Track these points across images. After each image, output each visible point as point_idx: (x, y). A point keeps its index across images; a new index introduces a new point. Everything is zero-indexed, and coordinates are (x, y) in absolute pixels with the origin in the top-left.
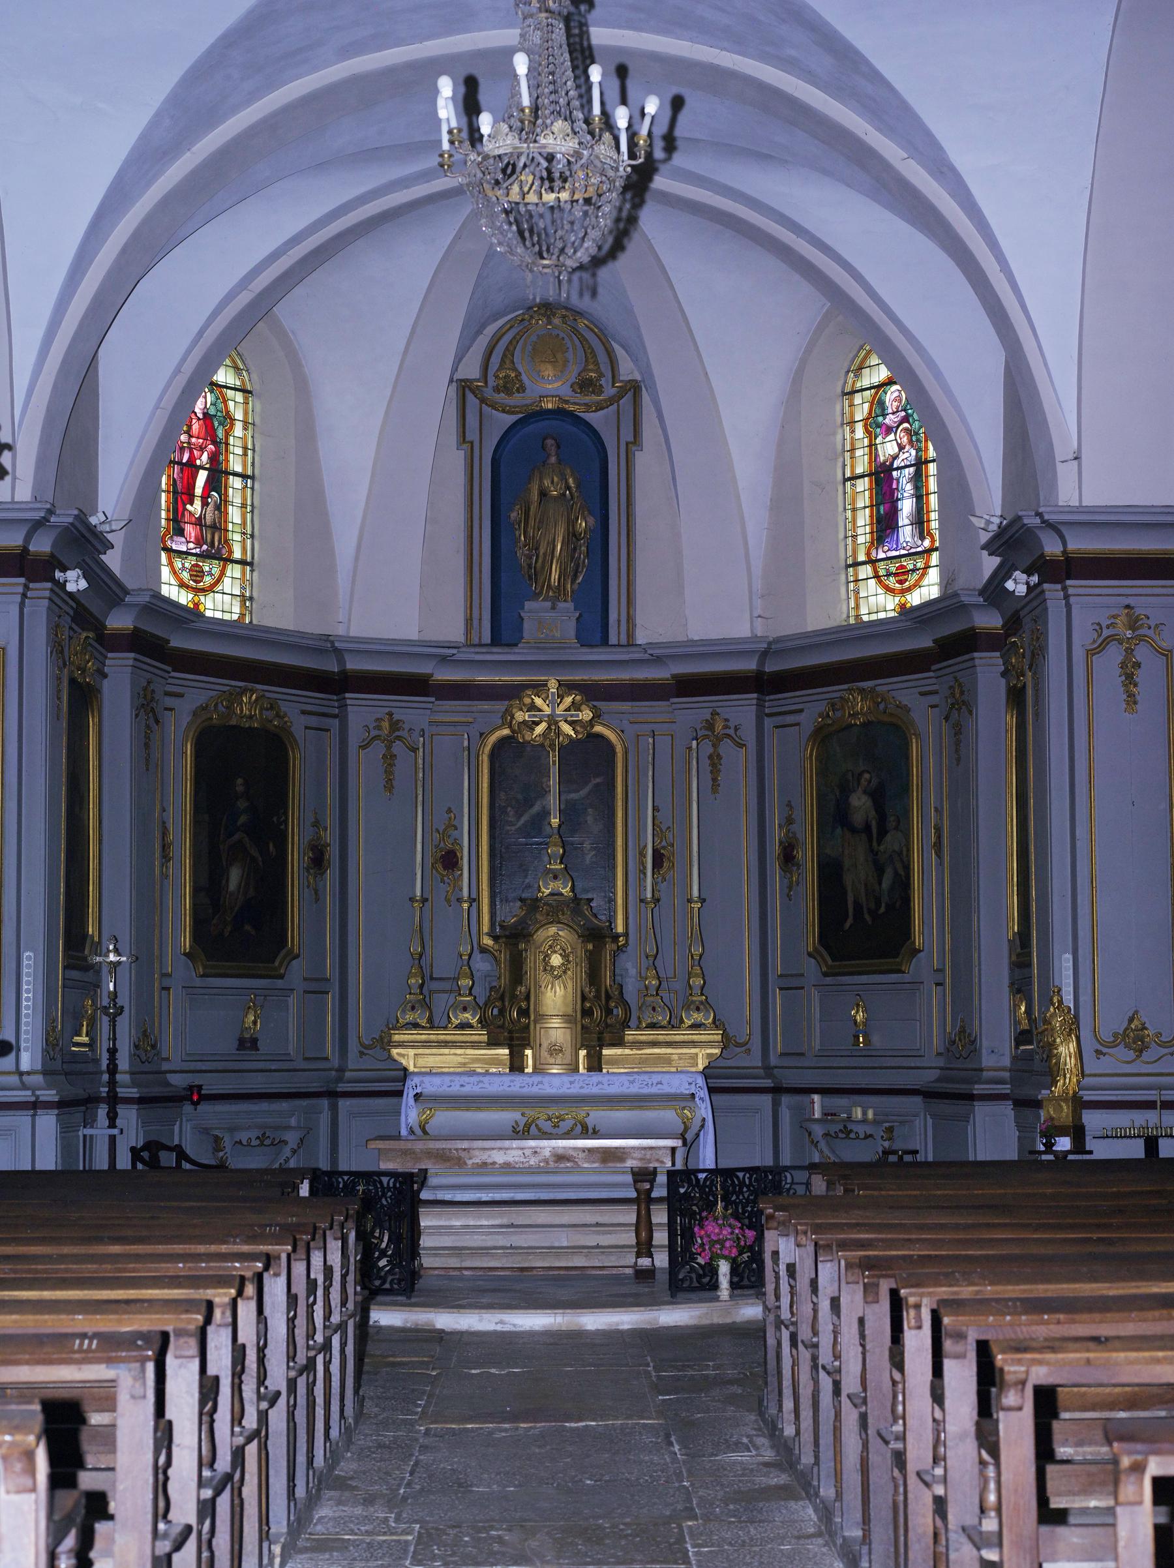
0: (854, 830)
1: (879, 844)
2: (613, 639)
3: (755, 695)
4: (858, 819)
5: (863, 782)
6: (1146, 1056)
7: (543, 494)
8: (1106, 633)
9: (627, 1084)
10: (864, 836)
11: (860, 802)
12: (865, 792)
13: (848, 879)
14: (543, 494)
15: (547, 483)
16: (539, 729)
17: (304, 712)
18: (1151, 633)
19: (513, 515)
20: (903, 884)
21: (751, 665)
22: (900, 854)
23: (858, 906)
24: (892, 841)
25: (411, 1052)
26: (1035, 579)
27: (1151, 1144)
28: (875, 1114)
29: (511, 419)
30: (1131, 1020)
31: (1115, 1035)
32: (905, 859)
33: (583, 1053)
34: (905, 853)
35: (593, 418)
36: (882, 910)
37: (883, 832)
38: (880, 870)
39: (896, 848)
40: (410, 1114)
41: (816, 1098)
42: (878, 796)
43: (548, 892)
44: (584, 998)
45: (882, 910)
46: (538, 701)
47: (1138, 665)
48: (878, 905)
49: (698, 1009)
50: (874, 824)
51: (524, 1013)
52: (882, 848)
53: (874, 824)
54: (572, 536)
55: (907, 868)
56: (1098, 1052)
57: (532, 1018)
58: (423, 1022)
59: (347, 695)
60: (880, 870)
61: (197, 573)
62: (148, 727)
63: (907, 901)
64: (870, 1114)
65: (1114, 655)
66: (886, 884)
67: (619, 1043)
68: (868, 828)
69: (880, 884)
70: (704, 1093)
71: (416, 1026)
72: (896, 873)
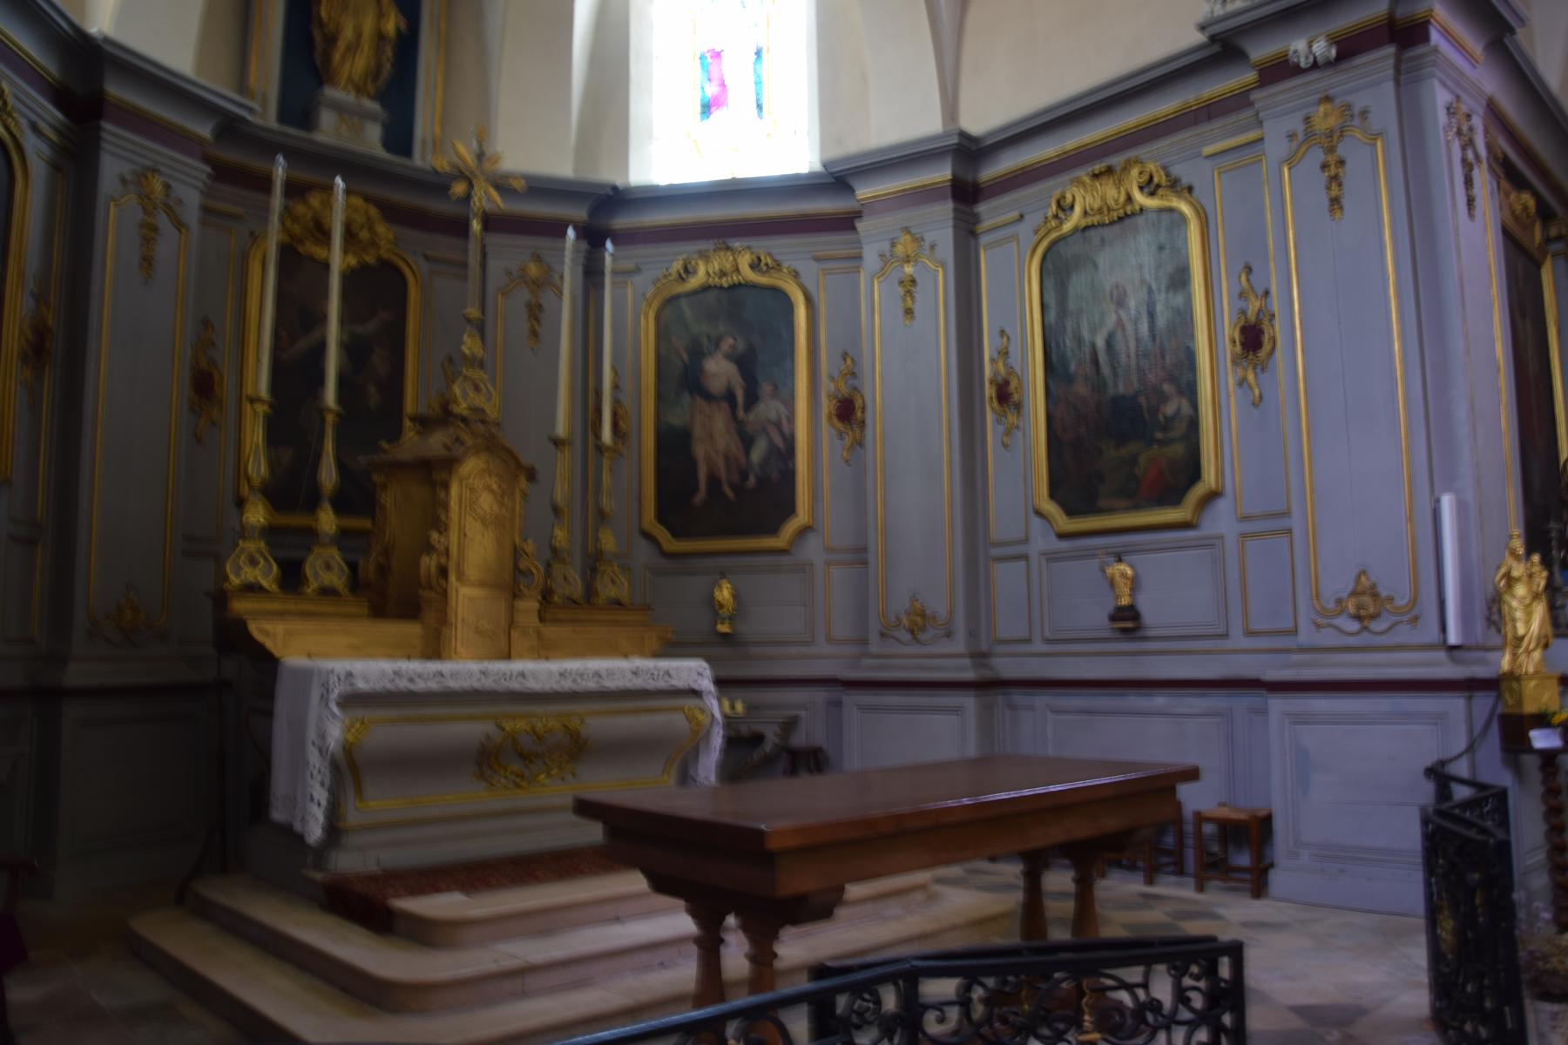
0: (708, 397)
4: (716, 385)
9: (629, 675)
10: (725, 405)
11: (719, 370)
12: (729, 357)
13: (700, 451)
22: (778, 425)
23: (714, 480)
24: (768, 408)
32: (786, 429)
34: (784, 422)
36: (752, 480)
37: (752, 398)
38: (747, 442)
39: (773, 416)
42: (746, 364)
45: (752, 480)
48: (744, 475)
52: (752, 417)
54: (381, 36)
55: (790, 442)
57: (452, 578)
63: (789, 476)
64: (739, 707)
66: (757, 454)
68: (730, 397)
69: (747, 452)
72: (771, 442)
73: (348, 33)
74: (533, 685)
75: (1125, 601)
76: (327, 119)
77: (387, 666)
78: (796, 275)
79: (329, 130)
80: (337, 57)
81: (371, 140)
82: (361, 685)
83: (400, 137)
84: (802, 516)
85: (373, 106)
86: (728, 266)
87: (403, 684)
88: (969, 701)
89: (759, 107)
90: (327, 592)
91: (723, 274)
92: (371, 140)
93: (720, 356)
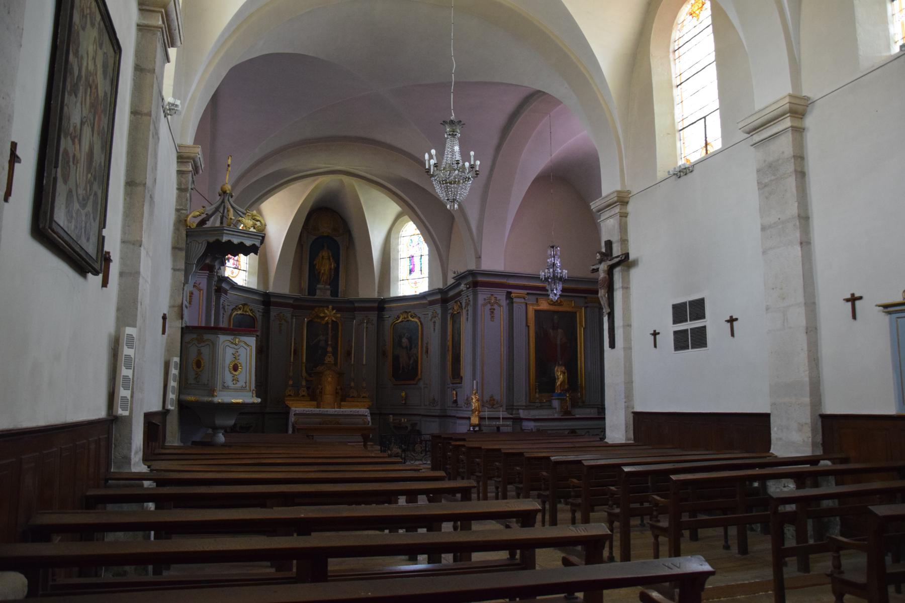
1: (410, 350)
2: (339, 295)
3: (377, 312)
5: (406, 336)
6: (494, 407)
7: (323, 257)
8: (487, 301)
11: (404, 340)
14: (323, 257)
15: (324, 254)
16: (327, 319)
17: (259, 311)
18: (497, 301)
19: (315, 262)
20: (416, 362)
21: (376, 305)
25: (291, 402)
26: (468, 286)
27: (498, 428)
28: (407, 420)
29: (315, 237)
30: (490, 398)
31: (487, 402)
33: (336, 404)
35: (336, 239)
37: (410, 349)
38: (410, 358)
40: (292, 419)
41: (391, 416)
43: (327, 361)
44: (337, 389)
46: (326, 311)
47: (494, 309)
49: (364, 393)
50: (408, 346)
51: (321, 392)
53: (408, 346)
54: (330, 269)
55: (417, 358)
56: (483, 406)
58: (292, 395)
59: (271, 307)
60: (410, 358)
61: (233, 273)
62: (223, 314)
63: (417, 366)
64: (406, 420)
65: (489, 306)
66: (411, 362)
67: (345, 401)
68: (407, 347)
70: (369, 415)
71: (290, 395)
73: (322, 271)
74: (329, 413)
75: (455, 399)
76: (318, 292)
77: (302, 409)
78: (419, 318)
79: (319, 295)
80: (321, 276)
81: (328, 295)
82: (297, 412)
83: (335, 293)
84: (419, 376)
85: (328, 287)
86: (406, 317)
87: (305, 412)
88: (437, 419)
89: (421, 271)
90: (303, 396)
91: (405, 318)
92: (328, 295)
93: (405, 338)
